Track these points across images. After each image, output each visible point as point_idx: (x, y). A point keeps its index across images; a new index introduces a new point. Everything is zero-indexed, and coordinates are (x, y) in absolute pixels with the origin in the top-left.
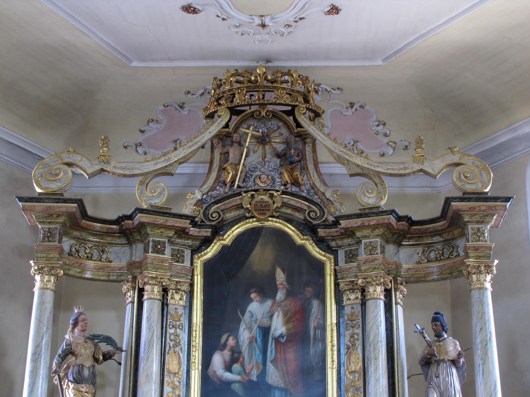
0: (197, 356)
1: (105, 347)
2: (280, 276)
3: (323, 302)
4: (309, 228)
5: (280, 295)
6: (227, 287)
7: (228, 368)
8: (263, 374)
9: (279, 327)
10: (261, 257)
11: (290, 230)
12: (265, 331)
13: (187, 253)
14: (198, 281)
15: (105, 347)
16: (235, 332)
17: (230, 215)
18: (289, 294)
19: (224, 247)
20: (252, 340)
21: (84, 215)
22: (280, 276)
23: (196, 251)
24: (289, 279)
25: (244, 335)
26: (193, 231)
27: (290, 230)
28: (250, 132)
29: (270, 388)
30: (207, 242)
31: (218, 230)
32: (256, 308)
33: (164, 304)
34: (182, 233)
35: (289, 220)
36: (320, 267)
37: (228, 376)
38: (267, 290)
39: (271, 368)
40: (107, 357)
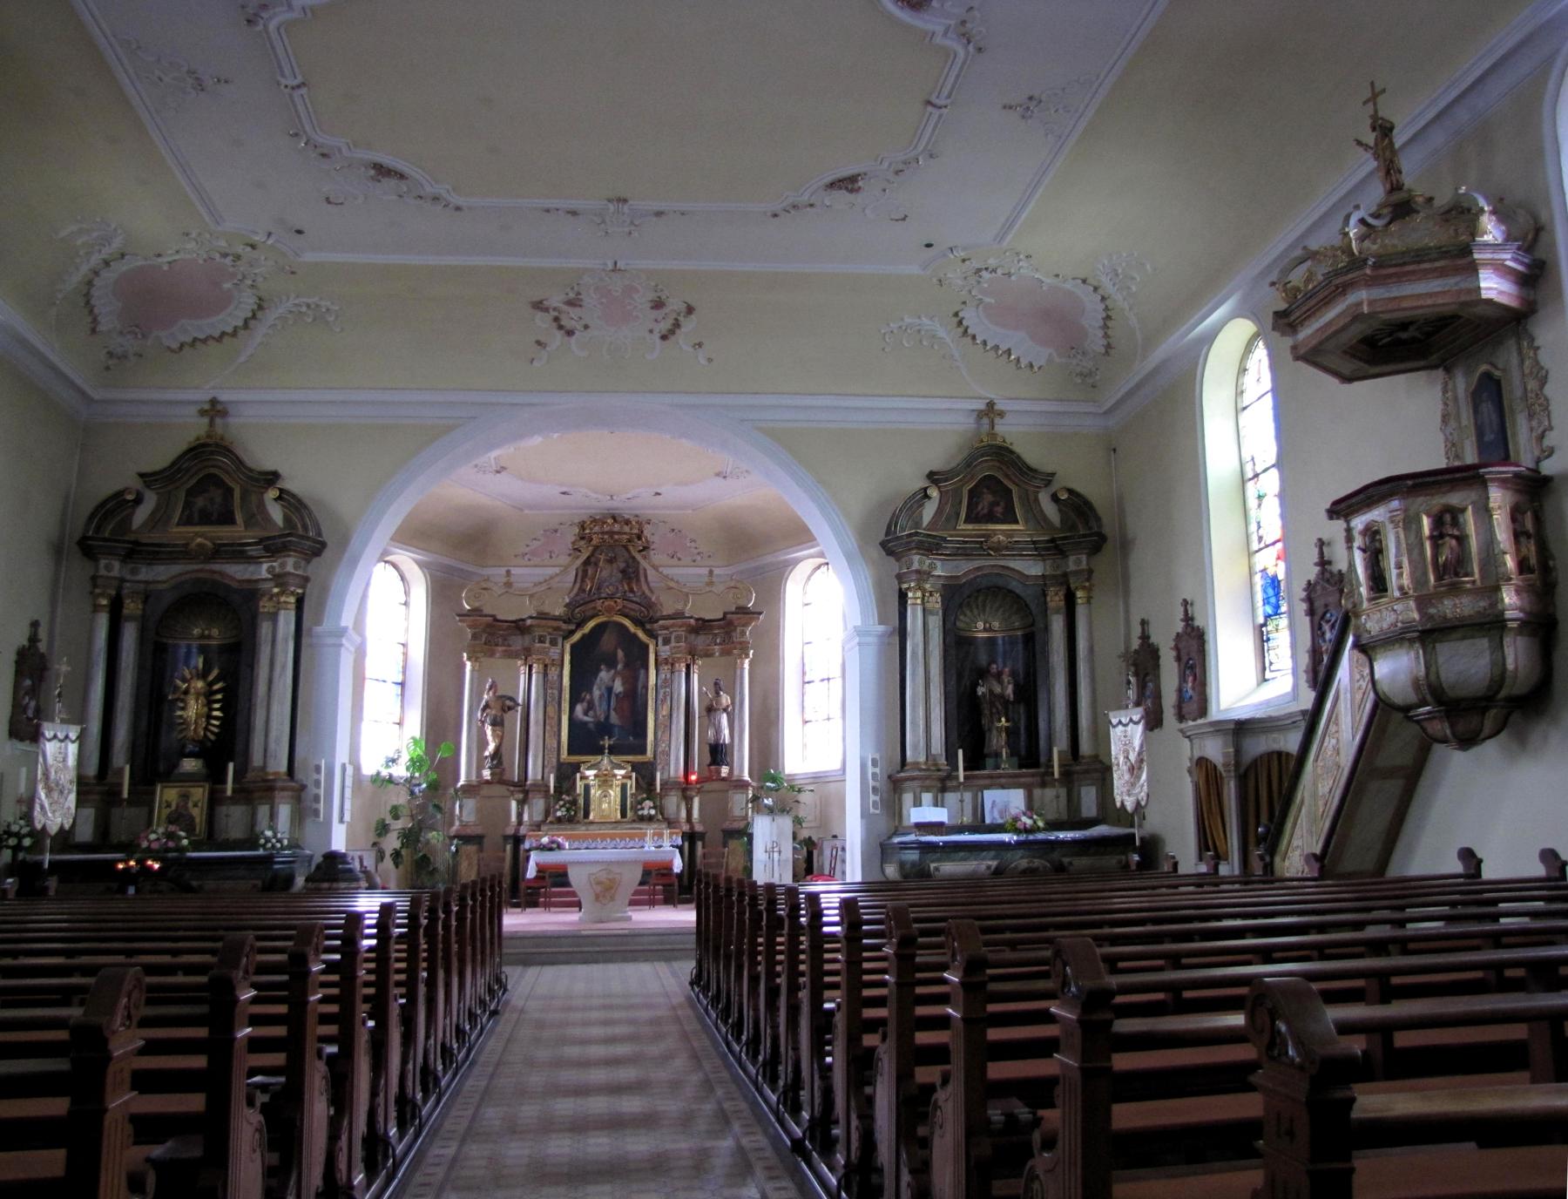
0: (566, 706)
1: (508, 703)
2: (620, 654)
3: (647, 669)
4: (638, 623)
5: (620, 667)
6: (586, 663)
7: (586, 714)
8: (607, 717)
9: (618, 687)
10: (608, 641)
11: (627, 623)
12: (610, 690)
13: (560, 641)
14: (567, 658)
15: (508, 703)
16: (590, 691)
17: (589, 613)
18: (626, 665)
19: (584, 636)
20: (601, 696)
21: (496, 620)
22: (620, 654)
23: (565, 638)
24: (626, 655)
25: (596, 693)
26: (564, 626)
27: (627, 623)
28: (602, 557)
29: (613, 726)
30: (572, 632)
31: (580, 625)
32: (604, 675)
33: (545, 674)
34: (557, 629)
35: (626, 616)
36: (647, 647)
37: (586, 719)
38: (611, 664)
39: (613, 713)
40: (510, 708)
